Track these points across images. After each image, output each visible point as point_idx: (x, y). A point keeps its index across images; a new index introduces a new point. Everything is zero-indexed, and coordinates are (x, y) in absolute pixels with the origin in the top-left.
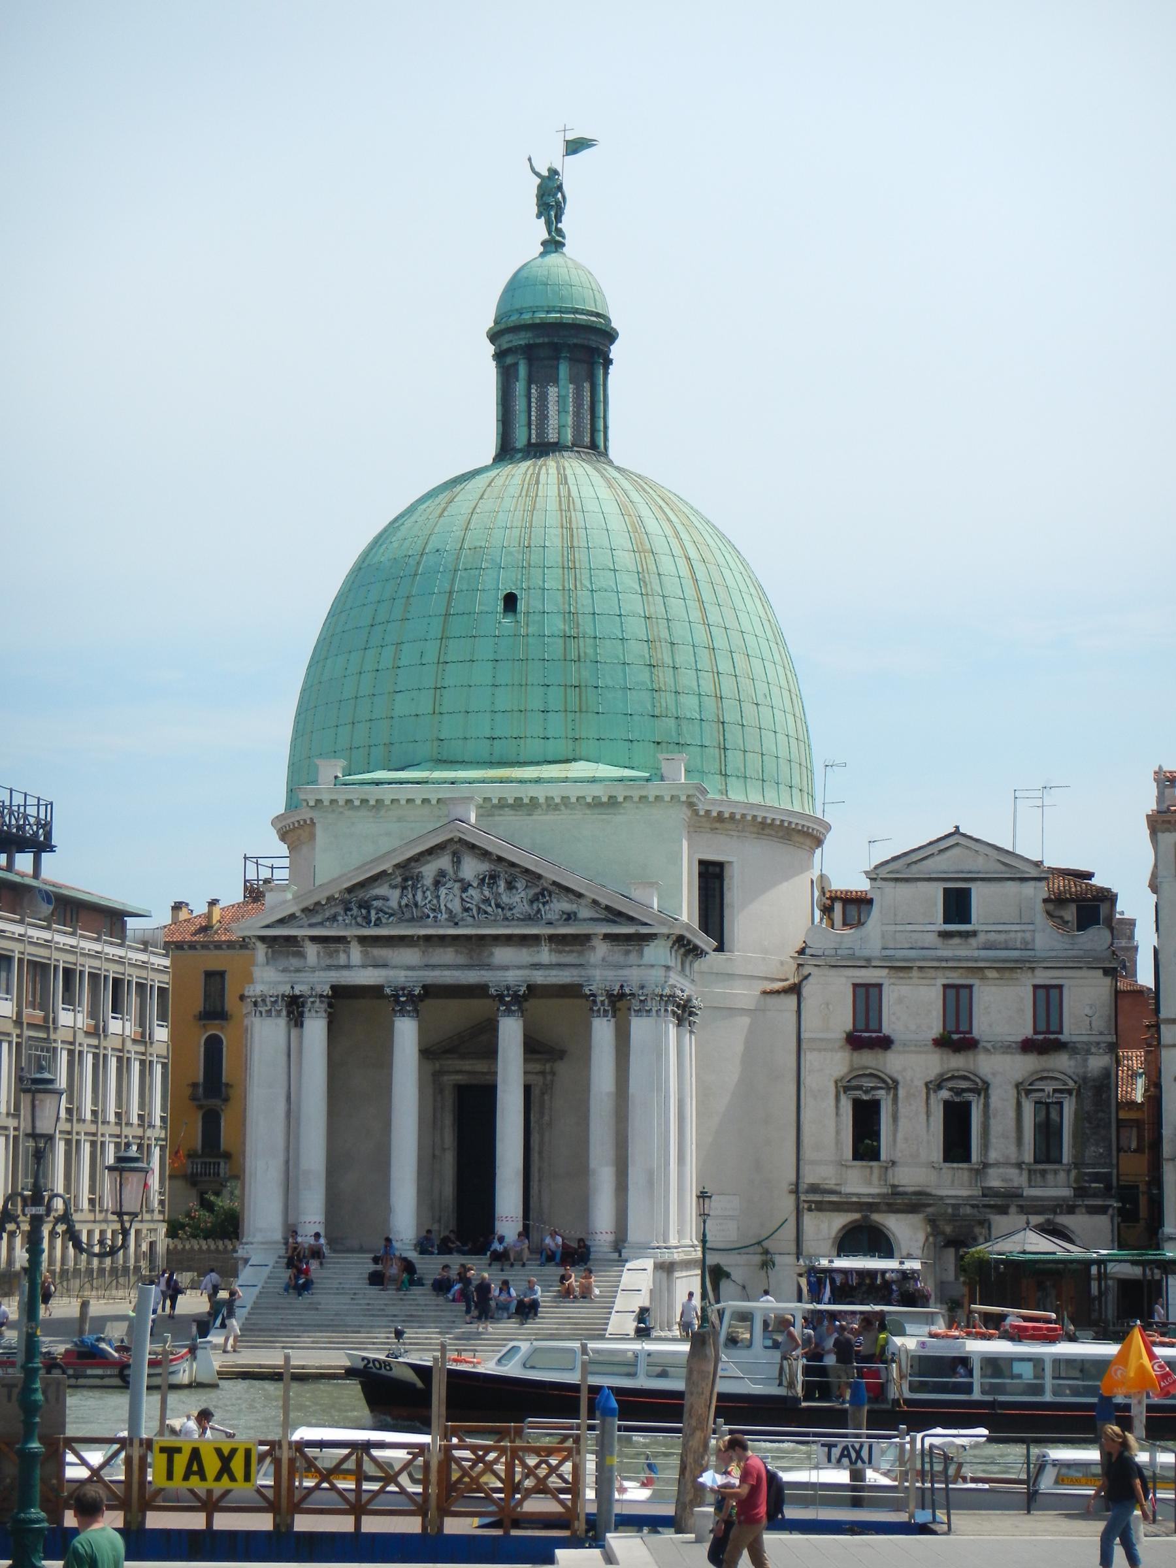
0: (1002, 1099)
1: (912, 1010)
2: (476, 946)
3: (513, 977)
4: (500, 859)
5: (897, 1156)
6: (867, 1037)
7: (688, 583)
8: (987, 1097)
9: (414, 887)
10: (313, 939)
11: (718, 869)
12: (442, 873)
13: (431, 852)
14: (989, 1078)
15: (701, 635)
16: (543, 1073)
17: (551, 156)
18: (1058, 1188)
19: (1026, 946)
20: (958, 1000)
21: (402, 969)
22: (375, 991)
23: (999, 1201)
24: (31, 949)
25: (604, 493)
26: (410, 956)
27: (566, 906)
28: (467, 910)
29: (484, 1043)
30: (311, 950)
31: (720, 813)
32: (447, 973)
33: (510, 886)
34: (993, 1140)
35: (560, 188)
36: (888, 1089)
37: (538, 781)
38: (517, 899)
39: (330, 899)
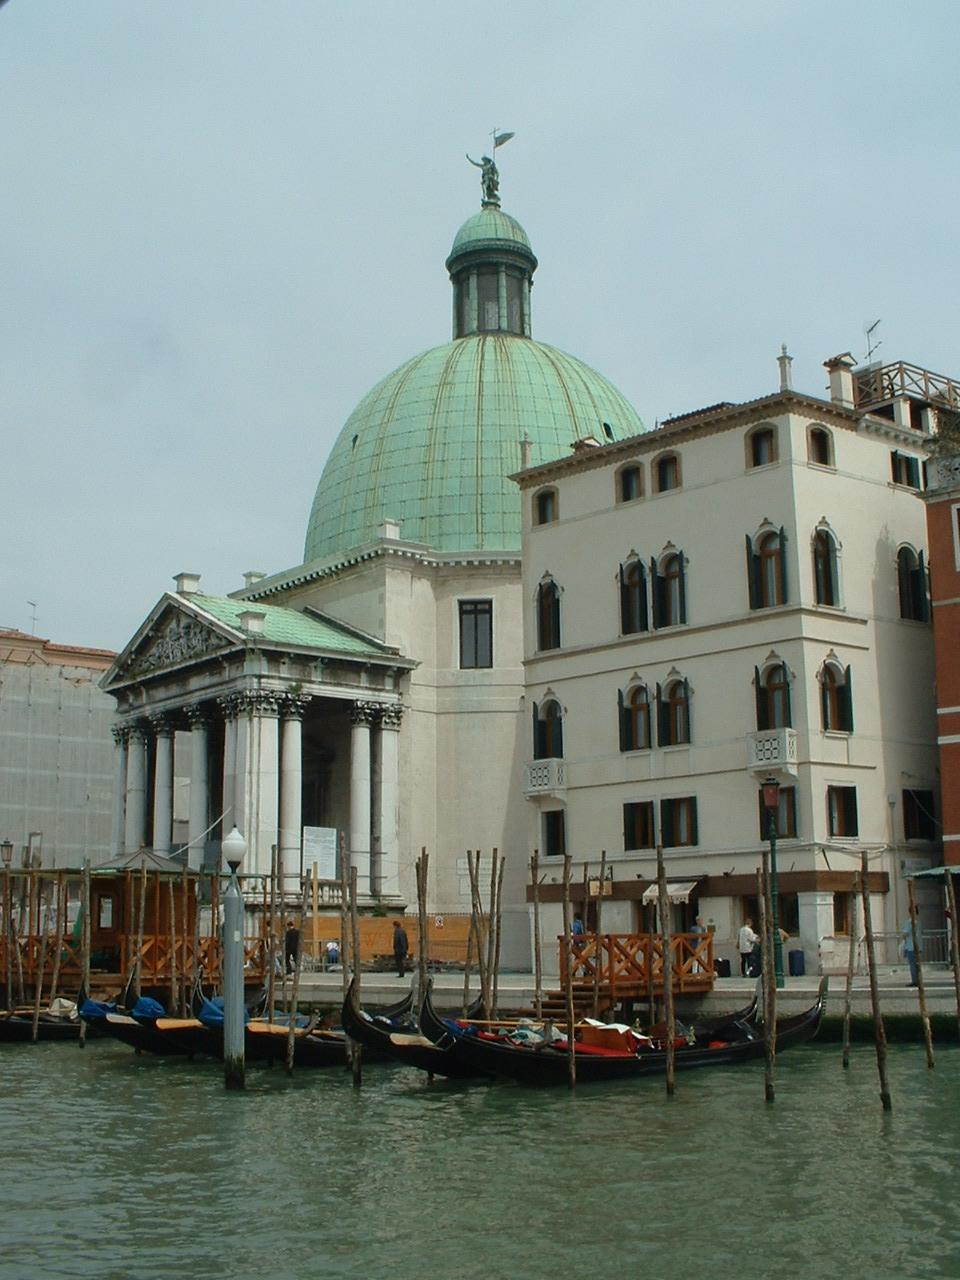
11: (487, 607)
26: (161, 693)
31: (470, 563)
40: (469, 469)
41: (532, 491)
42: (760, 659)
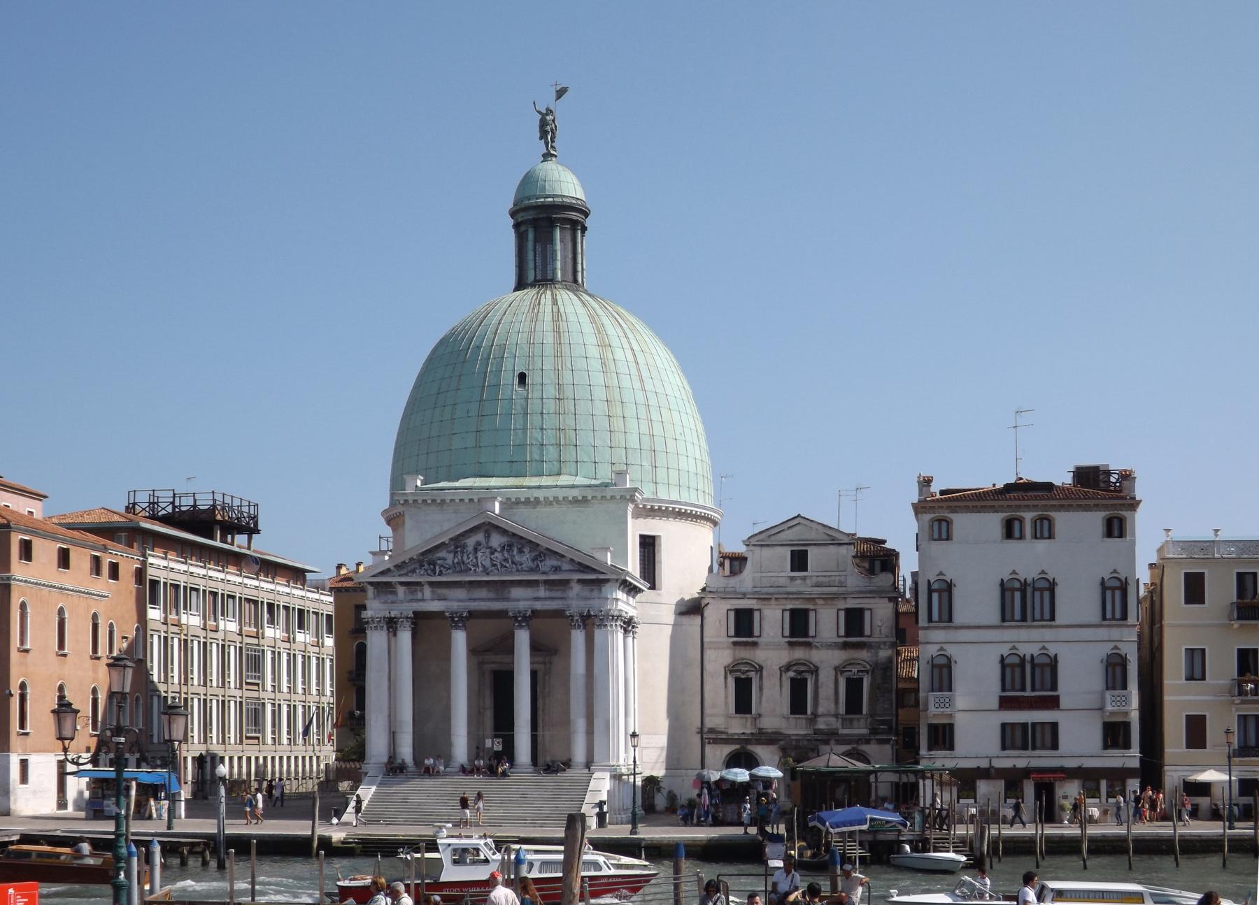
0: (826, 677)
1: (772, 622)
2: (501, 587)
3: (523, 605)
4: (514, 535)
5: (762, 711)
7: (632, 365)
8: (817, 676)
9: (462, 552)
10: (402, 583)
12: (479, 544)
14: (818, 664)
15: (640, 397)
16: (544, 663)
18: (860, 730)
19: (841, 585)
21: (456, 602)
22: (439, 615)
23: (824, 737)
24: (247, 591)
25: (581, 310)
26: (460, 593)
27: (555, 563)
29: (506, 646)
30: (401, 590)
33: (521, 551)
34: (821, 701)
36: (757, 671)
37: (539, 487)
39: (412, 559)
40: (644, 428)
41: (928, 517)
42: (1107, 649)
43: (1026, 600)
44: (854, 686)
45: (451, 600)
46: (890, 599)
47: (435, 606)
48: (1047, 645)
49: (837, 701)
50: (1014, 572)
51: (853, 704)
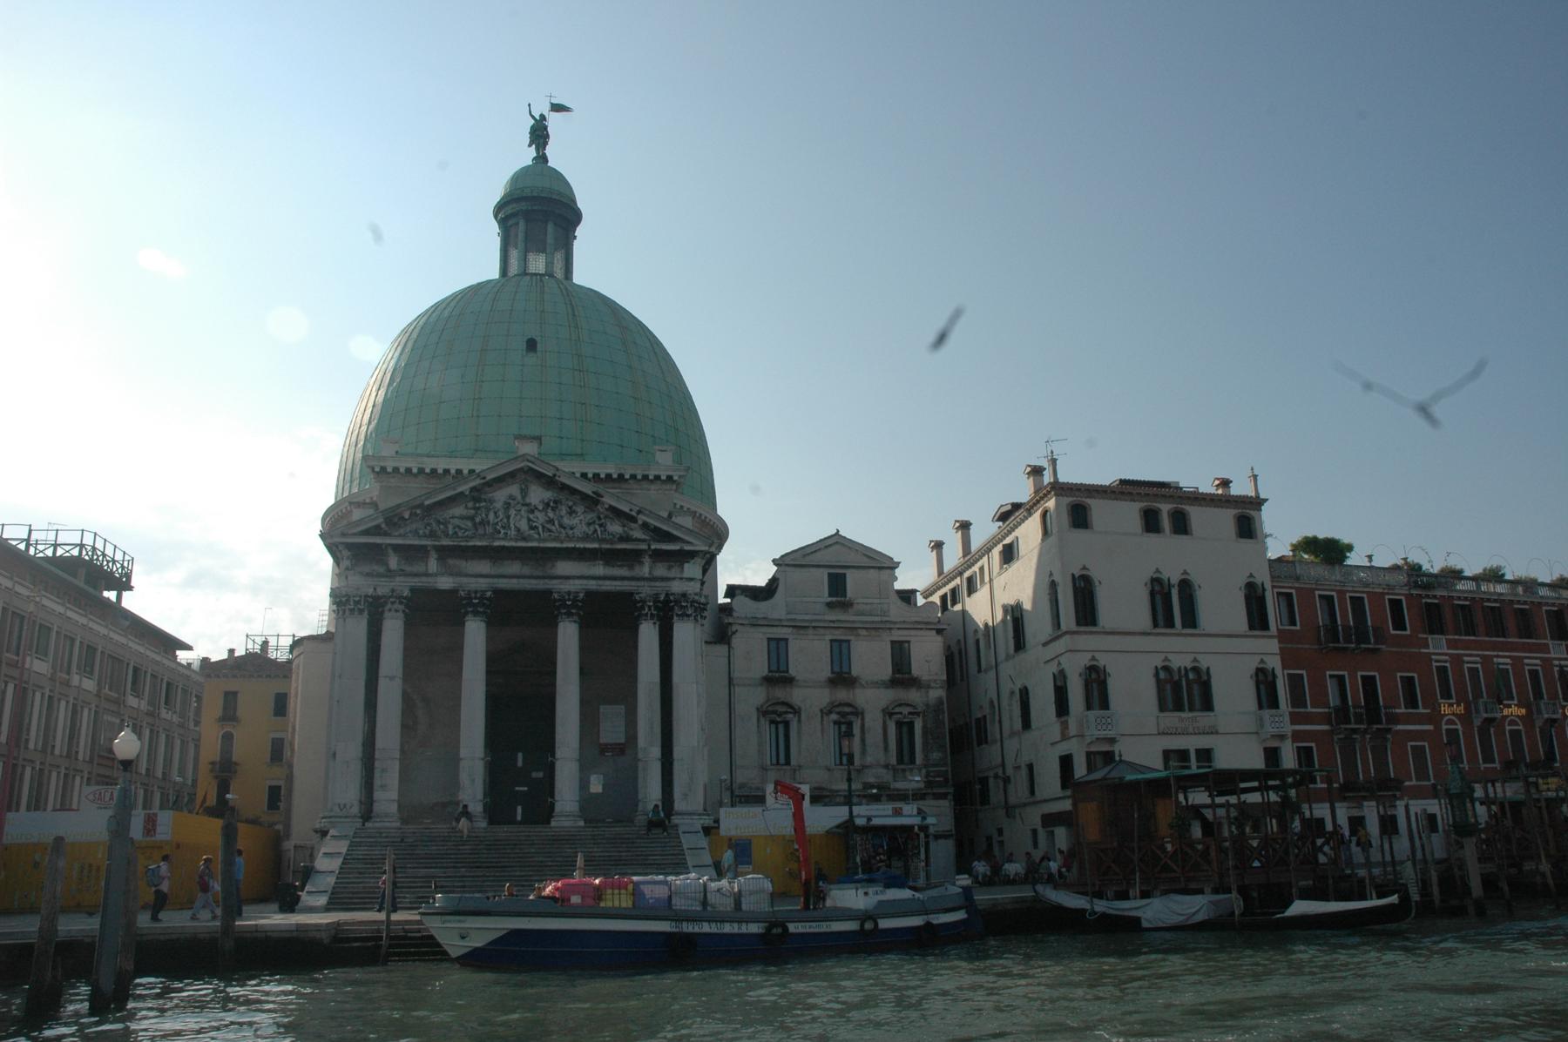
0: (874, 720)
1: (809, 658)
2: (542, 556)
6: (778, 677)
9: (488, 510)
10: (396, 548)
12: (511, 497)
13: (501, 481)
17: (541, 108)
20: (840, 650)
26: (484, 567)
28: (532, 528)
32: (515, 581)
33: (571, 512)
35: (546, 128)
38: (576, 521)
41: (1067, 500)
42: (1253, 663)
43: (1172, 604)
44: (905, 727)
45: (467, 575)
46: (939, 631)
47: (445, 583)
48: (1200, 657)
49: (886, 748)
50: (1157, 571)
51: (905, 755)
